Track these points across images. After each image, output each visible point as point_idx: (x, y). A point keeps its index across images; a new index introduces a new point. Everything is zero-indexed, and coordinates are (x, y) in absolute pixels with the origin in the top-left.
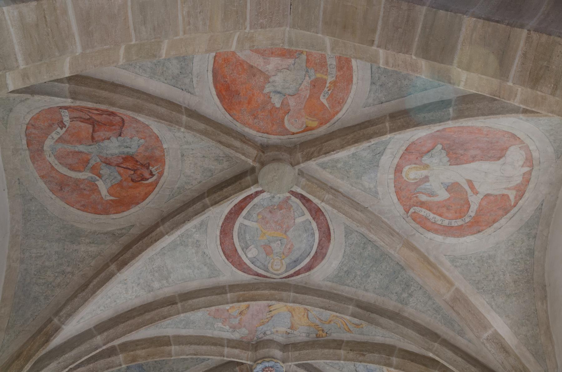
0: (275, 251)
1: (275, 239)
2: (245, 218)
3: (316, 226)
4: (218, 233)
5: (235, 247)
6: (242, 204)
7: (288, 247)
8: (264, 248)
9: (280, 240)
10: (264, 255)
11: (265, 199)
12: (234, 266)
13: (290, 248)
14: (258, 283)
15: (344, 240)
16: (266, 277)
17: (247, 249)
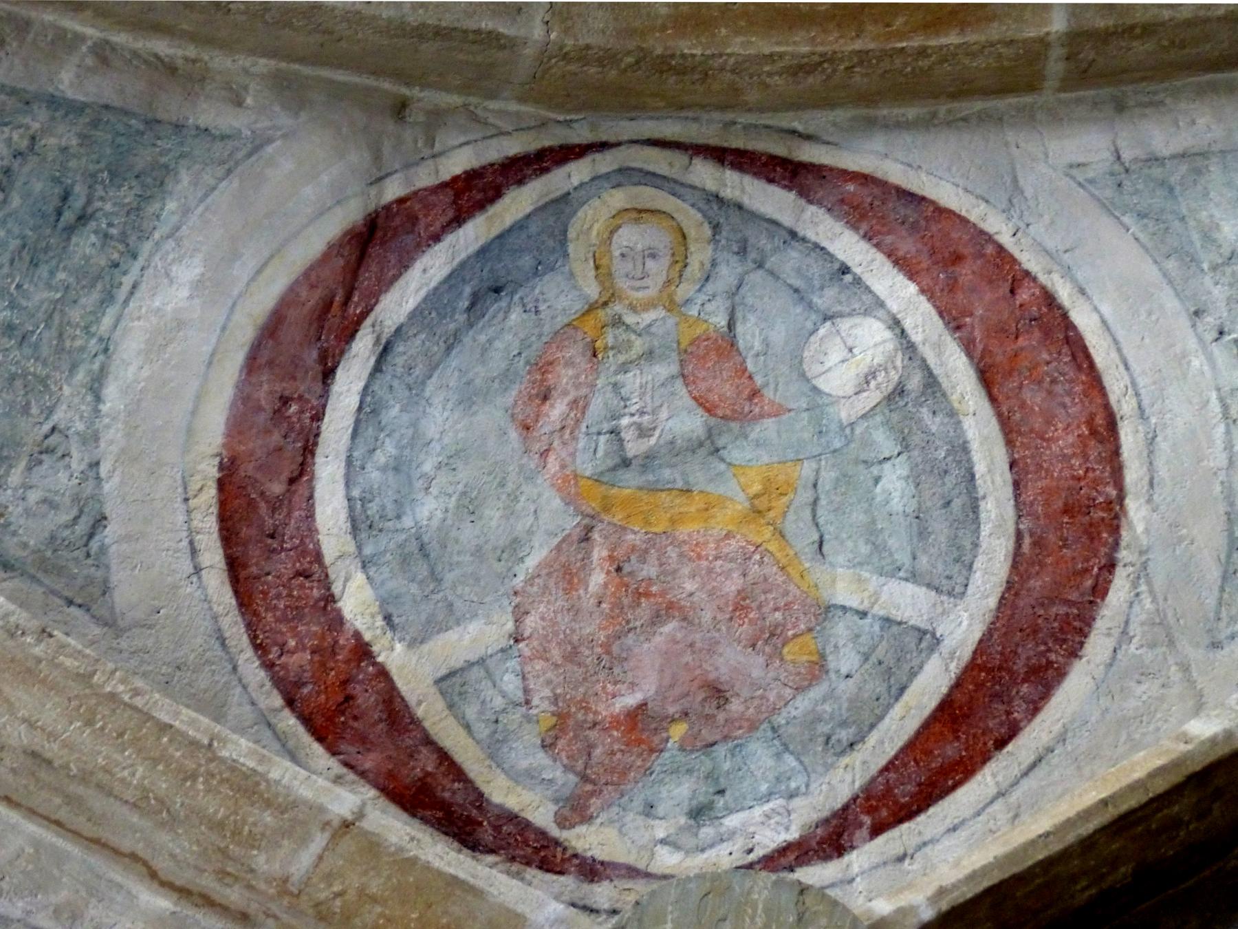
0: (664, 370)
1: (667, 473)
2: (927, 639)
3: (336, 589)
4: (1136, 512)
5: (993, 399)
6: (952, 750)
7: (557, 410)
8: (755, 393)
9: (626, 463)
10: (749, 334)
11: (768, 797)
12: (1001, 249)
13: (545, 398)
14: (797, 105)
15: (107, 487)
16: (720, 155)
17: (900, 391)
